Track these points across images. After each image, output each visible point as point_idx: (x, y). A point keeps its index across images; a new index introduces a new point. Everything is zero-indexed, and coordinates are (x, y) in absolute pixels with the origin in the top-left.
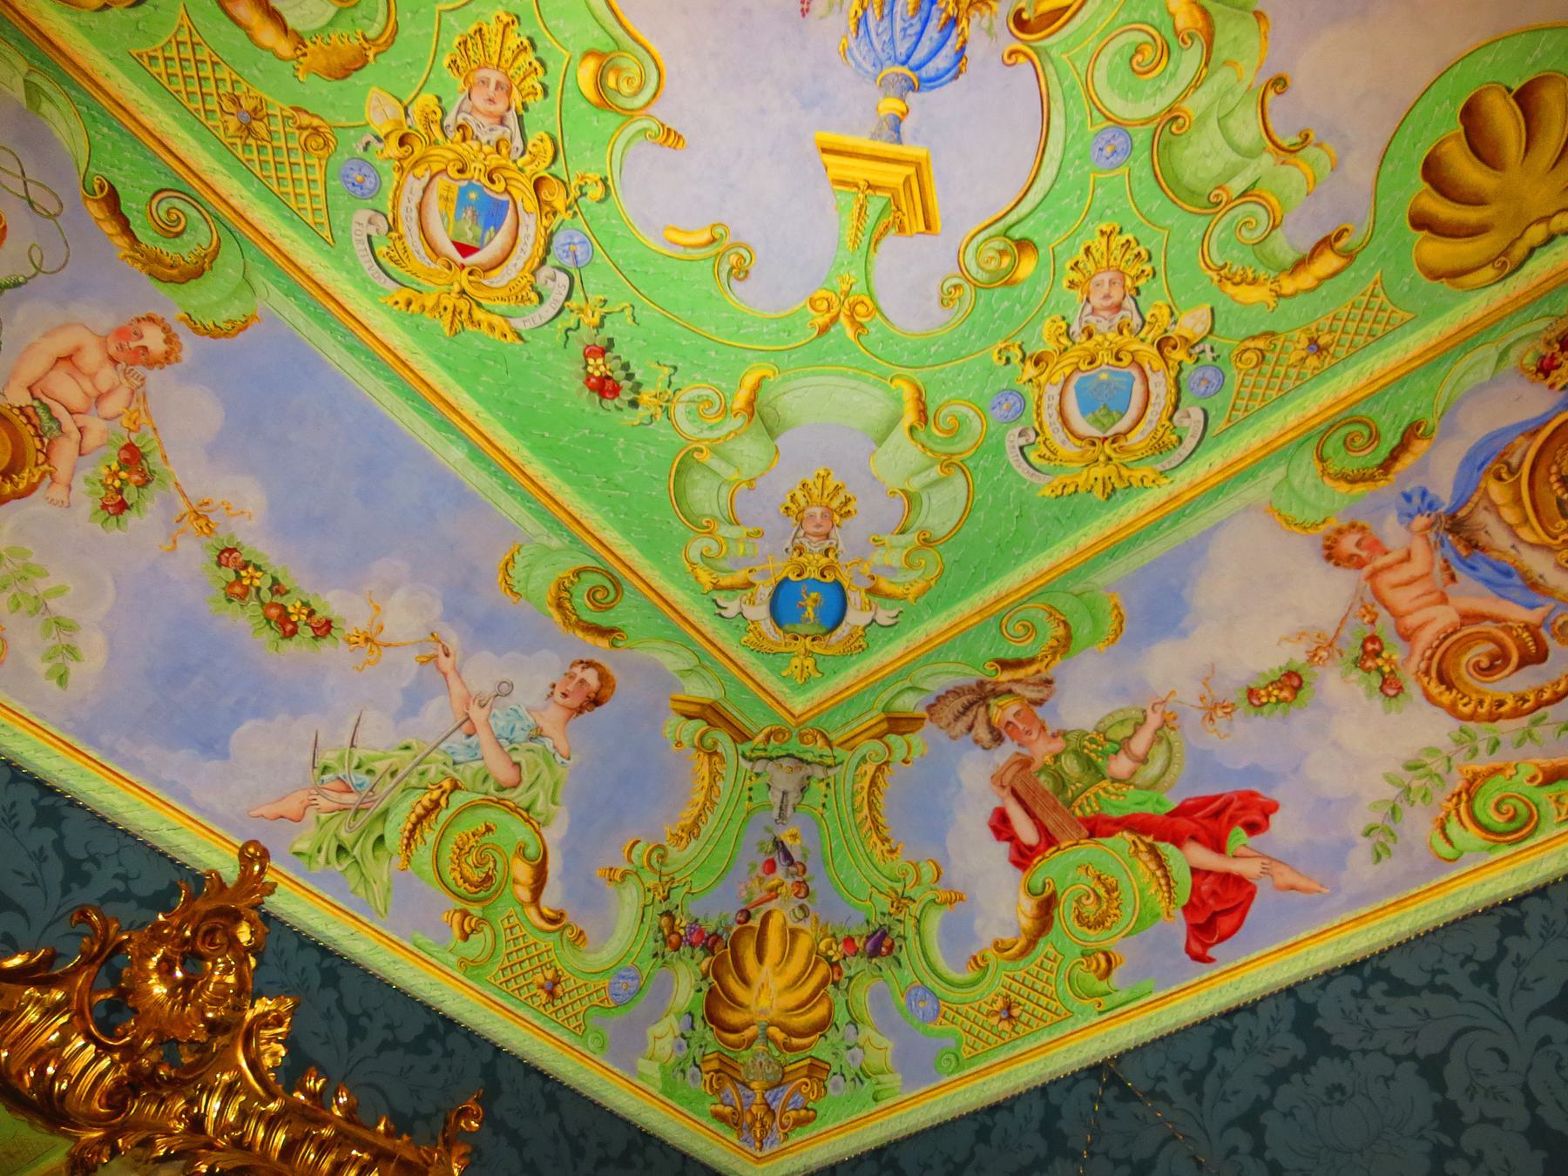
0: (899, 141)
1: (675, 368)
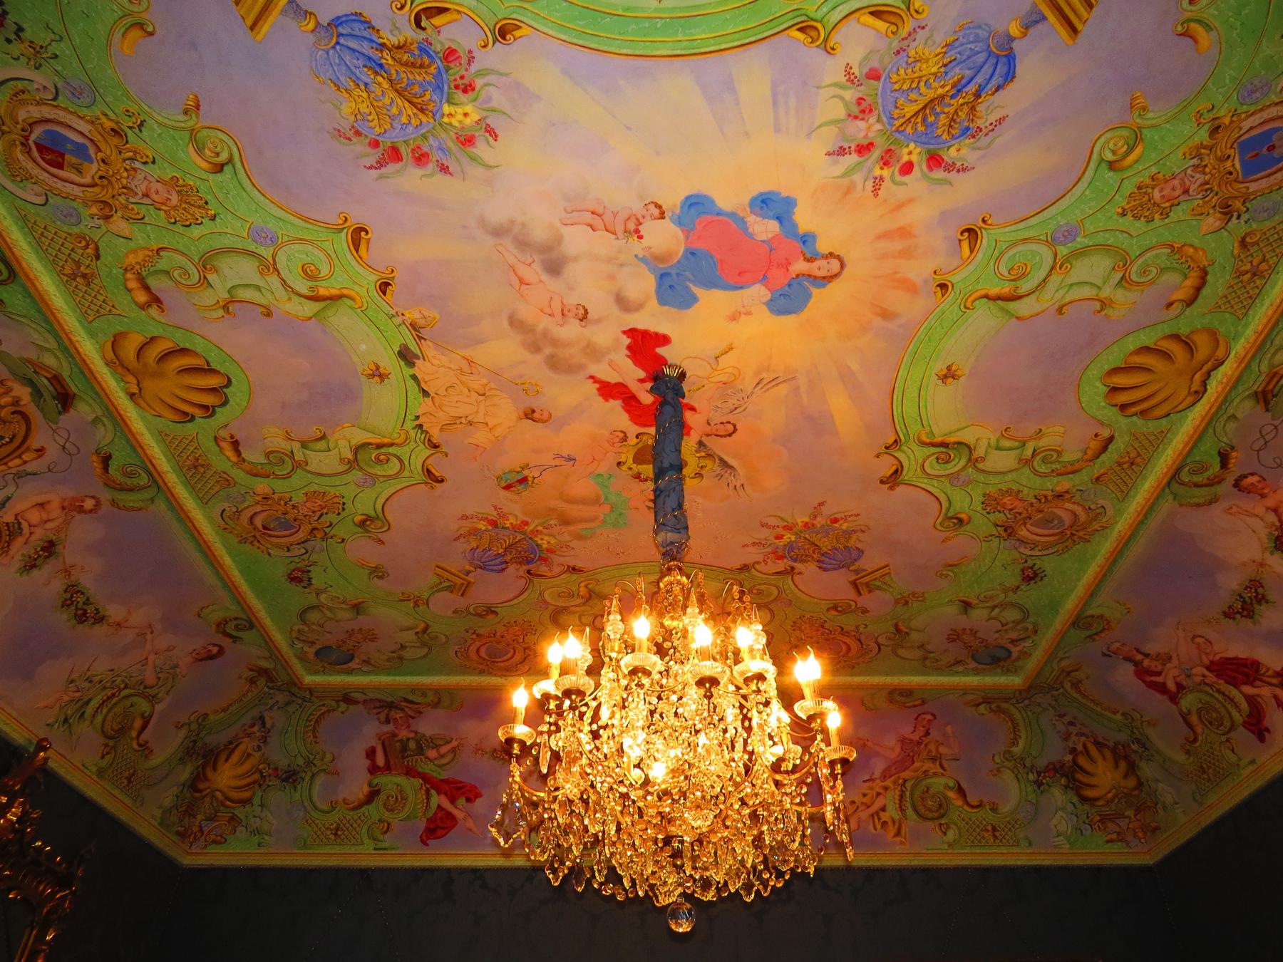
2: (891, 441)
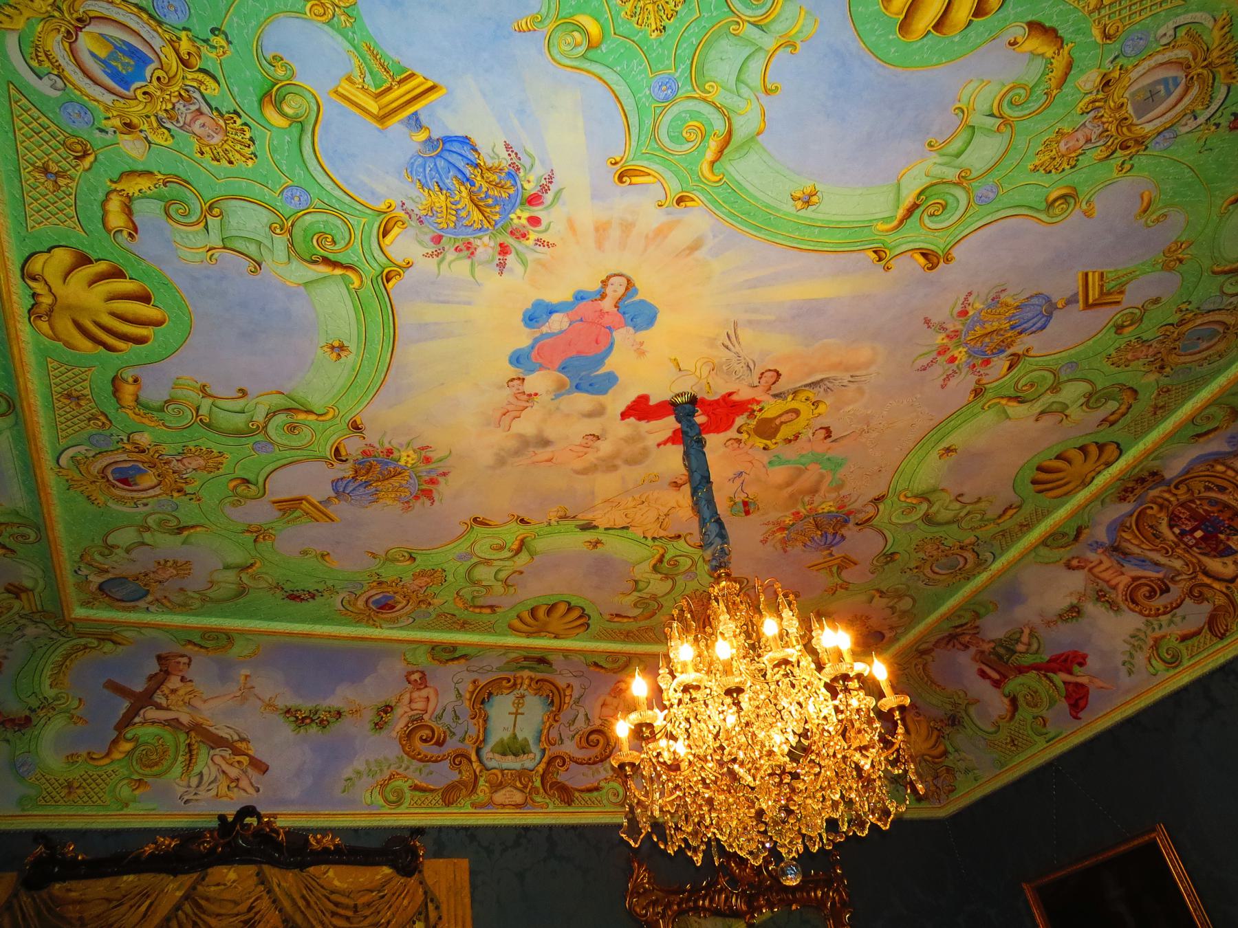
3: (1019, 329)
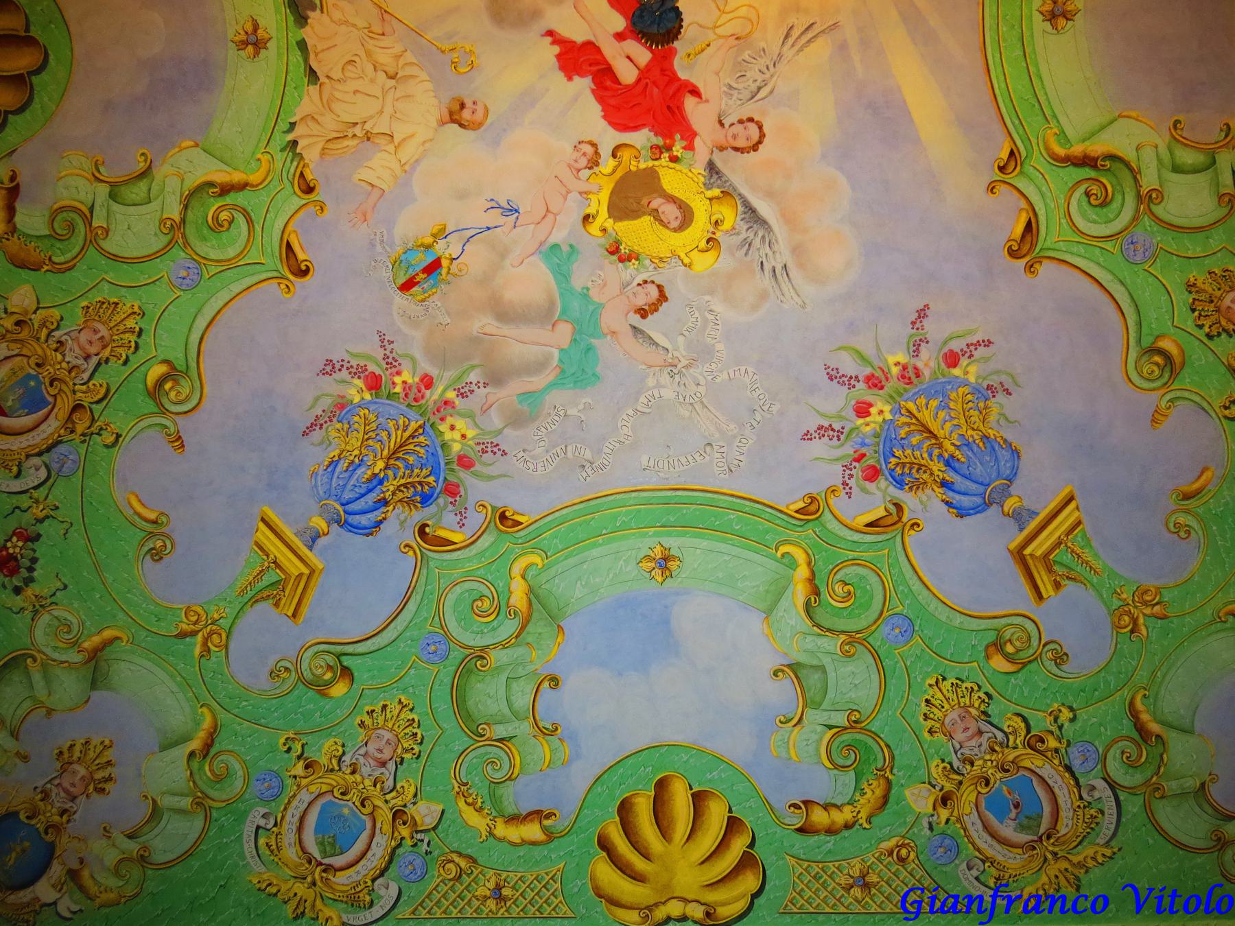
0: (310, 548)
1: (65, 587)
2: (1004, 155)
3: (950, 476)
